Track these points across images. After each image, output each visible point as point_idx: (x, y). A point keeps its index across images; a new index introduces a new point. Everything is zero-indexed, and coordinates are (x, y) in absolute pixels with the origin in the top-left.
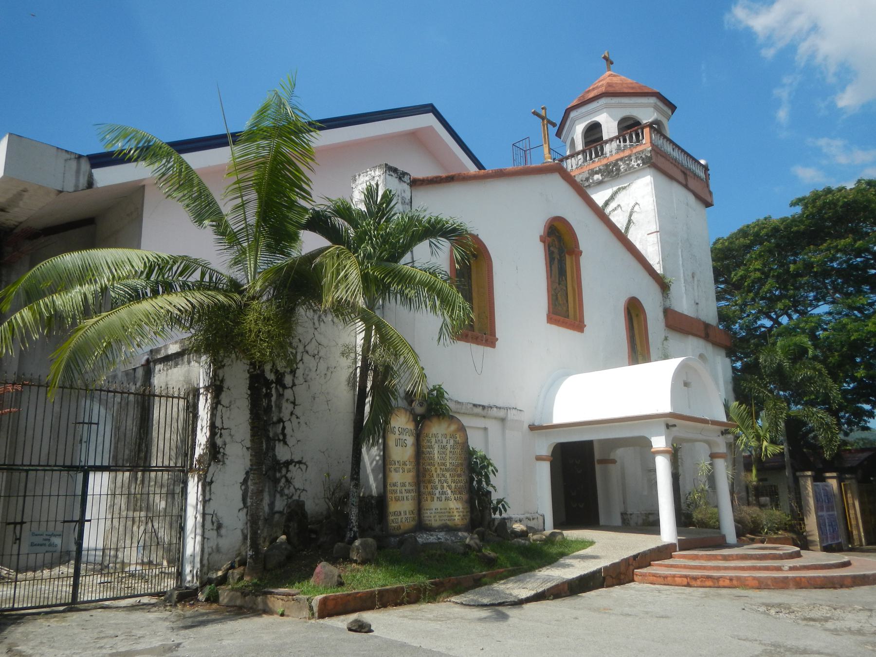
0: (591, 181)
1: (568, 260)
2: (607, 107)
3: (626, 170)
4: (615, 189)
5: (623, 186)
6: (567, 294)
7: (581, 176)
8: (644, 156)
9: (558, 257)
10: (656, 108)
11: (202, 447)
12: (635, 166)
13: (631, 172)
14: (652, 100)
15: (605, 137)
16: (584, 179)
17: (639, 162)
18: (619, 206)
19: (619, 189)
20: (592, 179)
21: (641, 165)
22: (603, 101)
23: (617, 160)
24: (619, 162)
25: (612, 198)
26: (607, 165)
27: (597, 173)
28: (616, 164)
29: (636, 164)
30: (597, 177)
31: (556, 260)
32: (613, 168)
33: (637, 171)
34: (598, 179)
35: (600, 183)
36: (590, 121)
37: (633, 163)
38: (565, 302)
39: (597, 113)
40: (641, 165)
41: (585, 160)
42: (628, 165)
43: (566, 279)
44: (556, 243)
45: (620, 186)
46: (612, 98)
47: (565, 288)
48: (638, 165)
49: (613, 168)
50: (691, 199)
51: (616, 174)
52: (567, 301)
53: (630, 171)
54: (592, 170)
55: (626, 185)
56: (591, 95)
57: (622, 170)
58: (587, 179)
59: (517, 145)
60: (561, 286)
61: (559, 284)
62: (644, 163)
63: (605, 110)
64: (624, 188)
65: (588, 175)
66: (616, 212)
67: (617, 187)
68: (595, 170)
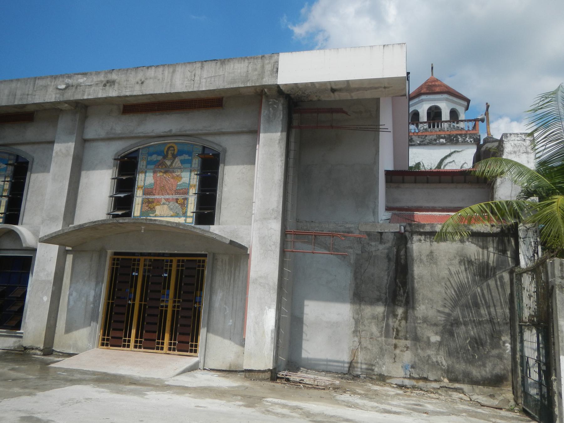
0: (438, 142)
2: (447, 100)
4: (453, 150)
5: (458, 150)
7: (431, 137)
8: (475, 137)
11: (532, 309)
12: (469, 141)
15: (443, 119)
16: (433, 139)
17: (472, 140)
18: (454, 161)
19: (455, 152)
20: (439, 141)
21: (473, 142)
22: (445, 96)
23: (457, 135)
24: (458, 136)
25: (449, 155)
26: (449, 135)
27: (442, 138)
28: (456, 136)
29: (469, 140)
30: (442, 140)
32: (454, 138)
33: (469, 144)
34: (443, 142)
35: (442, 144)
36: (434, 105)
37: (467, 139)
39: (441, 101)
40: (473, 142)
41: (430, 127)
42: (464, 139)
45: (456, 150)
48: (471, 141)
49: (454, 138)
51: (456, 143)
53: (465, 142)
54: (439, 135)
55: (459, 150)
56: (437, 89)
57: (460, 141)
58: (435, 140)
62: (474, 141)
63: (445, 101)
64: (458, 152)
65: (436, 138)
66: (451, 164)
67: (454, 150)
68: (441, 136)
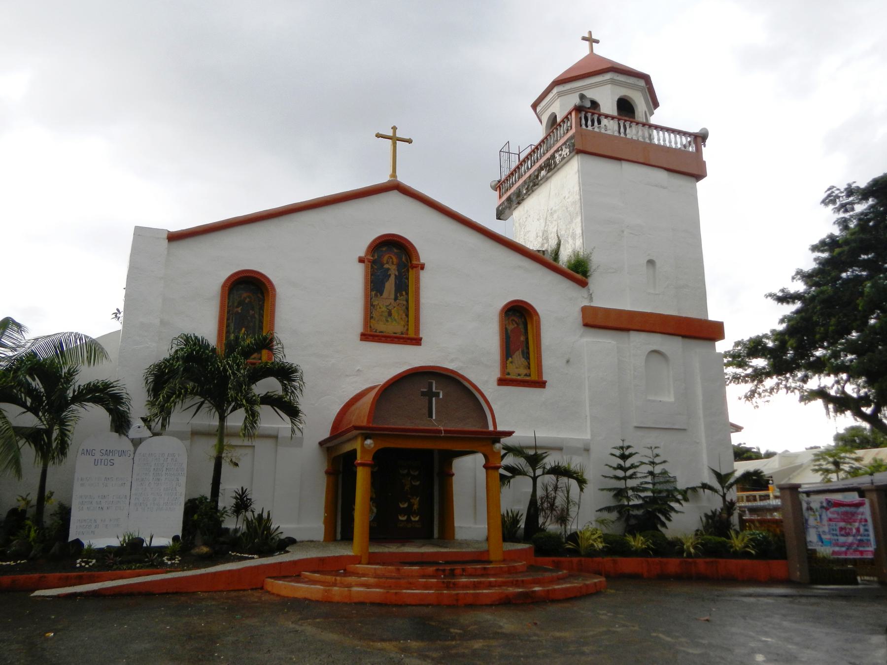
1: (412, 273)
3: (560, 162)
6: (407, 309)
9: (397, 274)
10: (613, 82)
13: (565, 161)
14: (608, 76)
31: (392, 279)
38: (404, 316)
43: (407, 294)
44: (395, 260)
46: (564, 85)
47: (405, 303)
50: (661, 176)
52: (407, 316)
59: (502, 150)
60: (398, 301)
61: (396, 299)
